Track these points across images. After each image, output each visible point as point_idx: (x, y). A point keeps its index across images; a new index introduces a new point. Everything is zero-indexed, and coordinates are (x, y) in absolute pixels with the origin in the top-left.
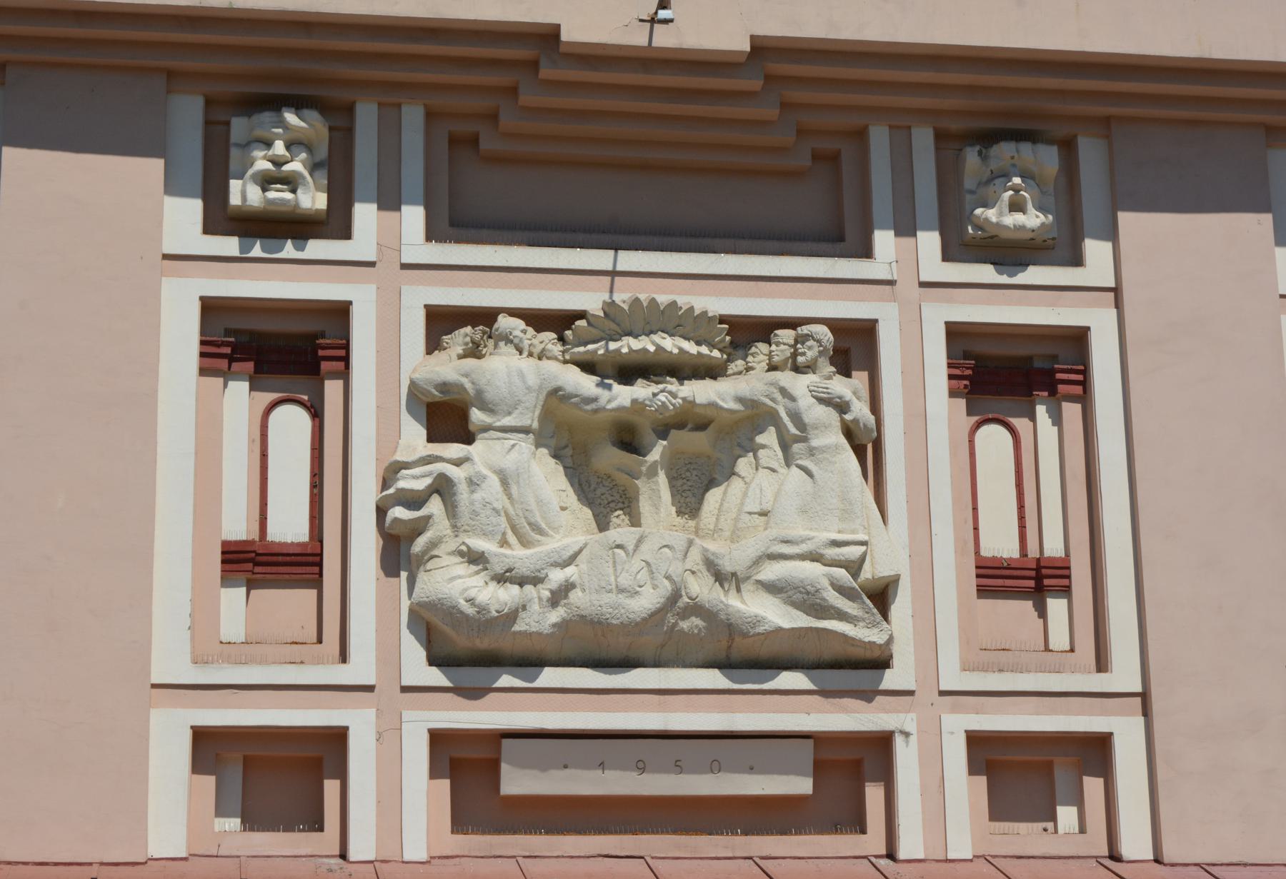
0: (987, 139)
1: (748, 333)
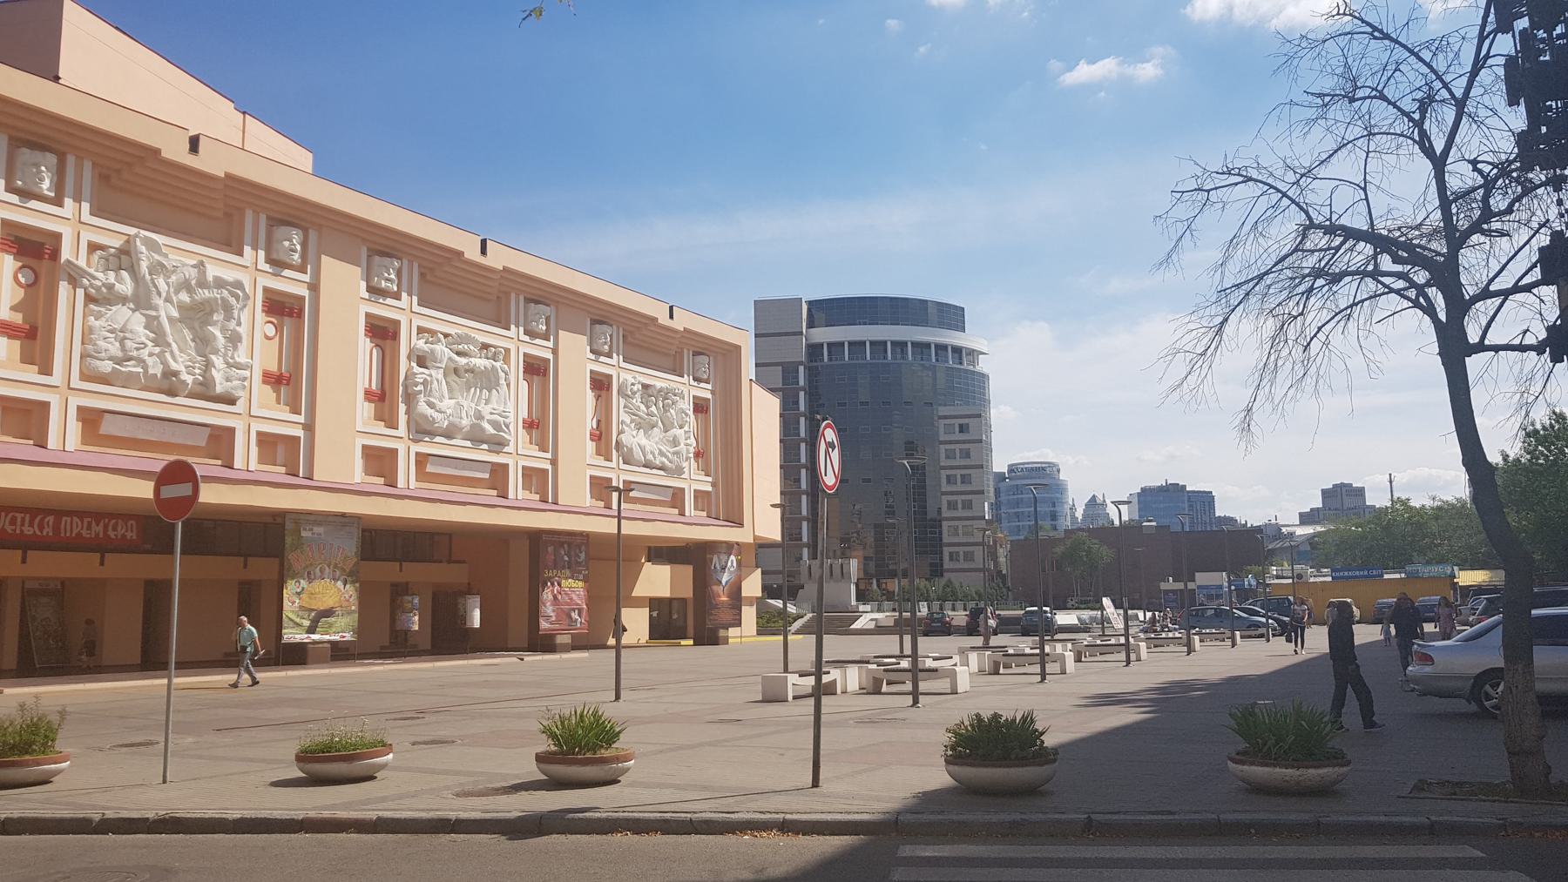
0: (537, 302)
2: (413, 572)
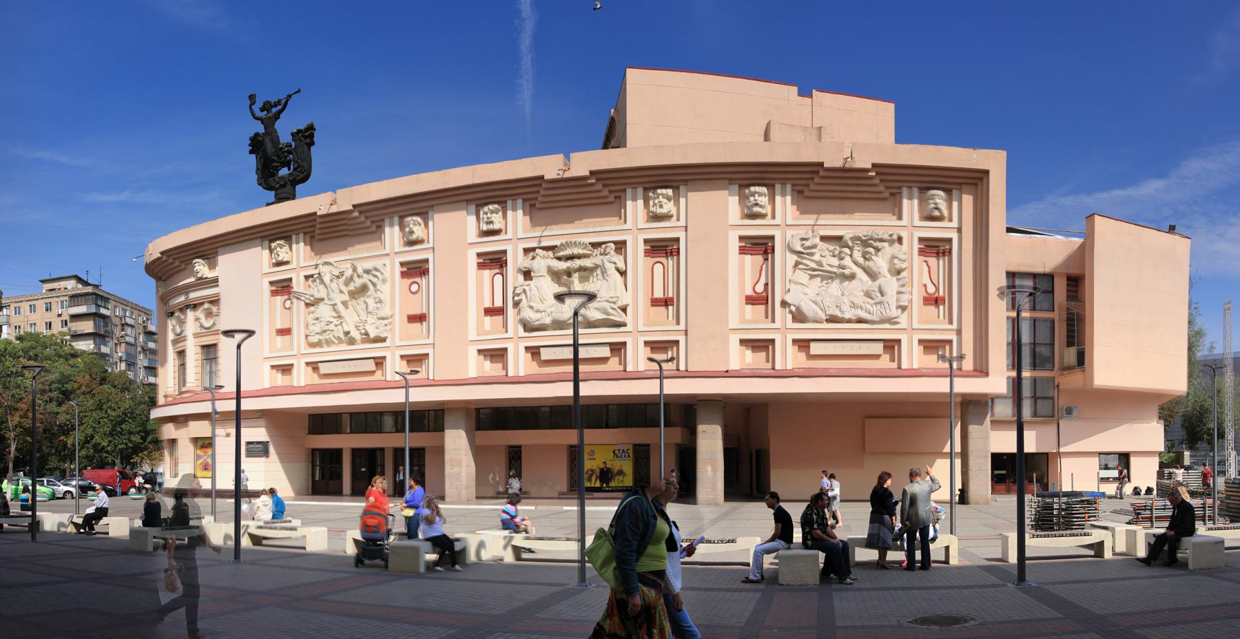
1: (595, 245)
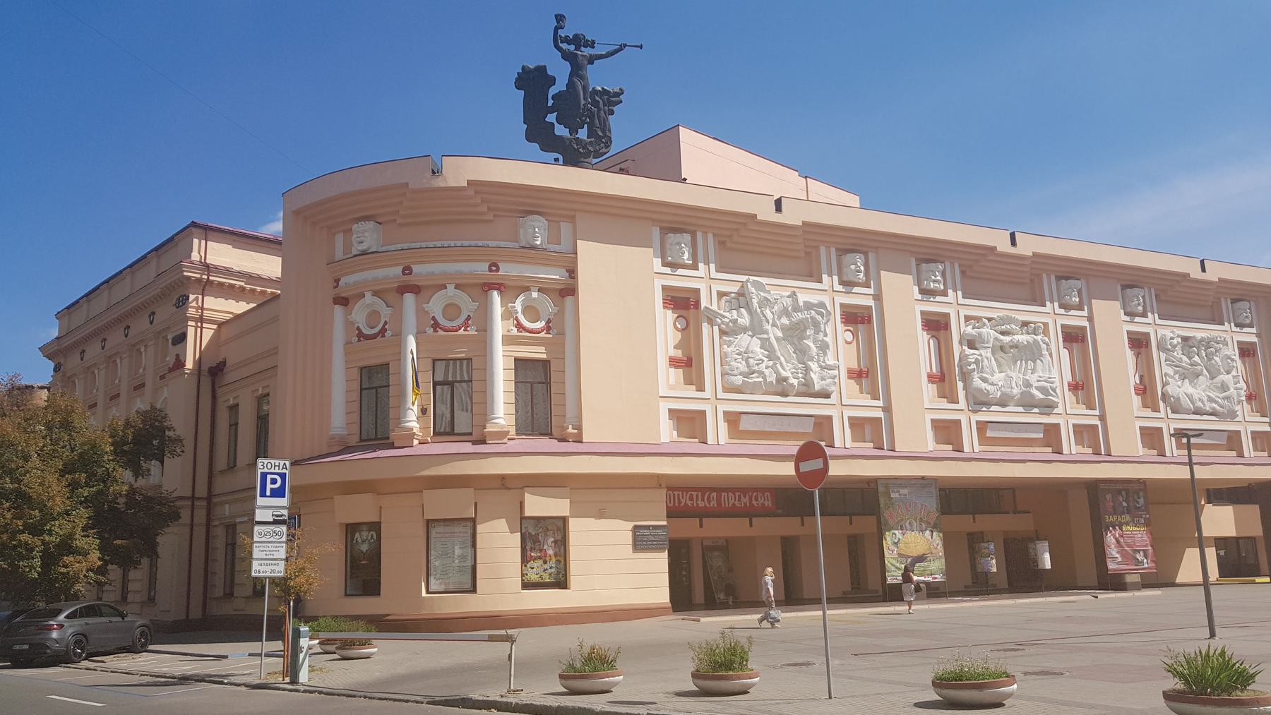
0: (1067, 278)
2: (986, 522)
